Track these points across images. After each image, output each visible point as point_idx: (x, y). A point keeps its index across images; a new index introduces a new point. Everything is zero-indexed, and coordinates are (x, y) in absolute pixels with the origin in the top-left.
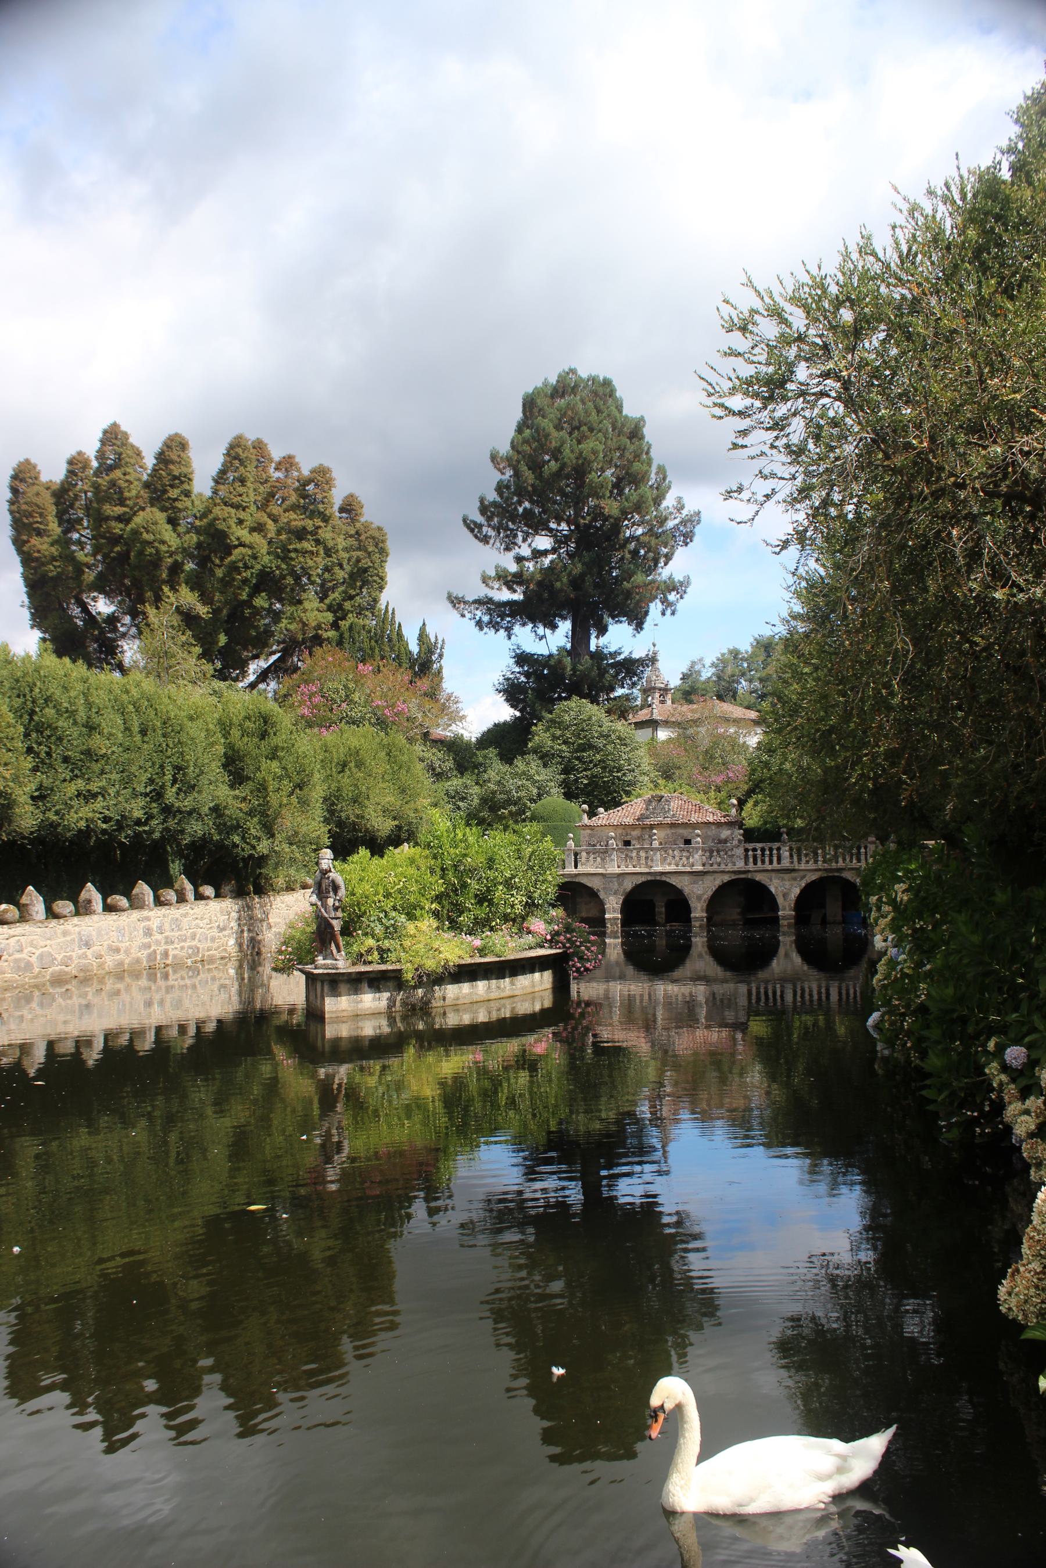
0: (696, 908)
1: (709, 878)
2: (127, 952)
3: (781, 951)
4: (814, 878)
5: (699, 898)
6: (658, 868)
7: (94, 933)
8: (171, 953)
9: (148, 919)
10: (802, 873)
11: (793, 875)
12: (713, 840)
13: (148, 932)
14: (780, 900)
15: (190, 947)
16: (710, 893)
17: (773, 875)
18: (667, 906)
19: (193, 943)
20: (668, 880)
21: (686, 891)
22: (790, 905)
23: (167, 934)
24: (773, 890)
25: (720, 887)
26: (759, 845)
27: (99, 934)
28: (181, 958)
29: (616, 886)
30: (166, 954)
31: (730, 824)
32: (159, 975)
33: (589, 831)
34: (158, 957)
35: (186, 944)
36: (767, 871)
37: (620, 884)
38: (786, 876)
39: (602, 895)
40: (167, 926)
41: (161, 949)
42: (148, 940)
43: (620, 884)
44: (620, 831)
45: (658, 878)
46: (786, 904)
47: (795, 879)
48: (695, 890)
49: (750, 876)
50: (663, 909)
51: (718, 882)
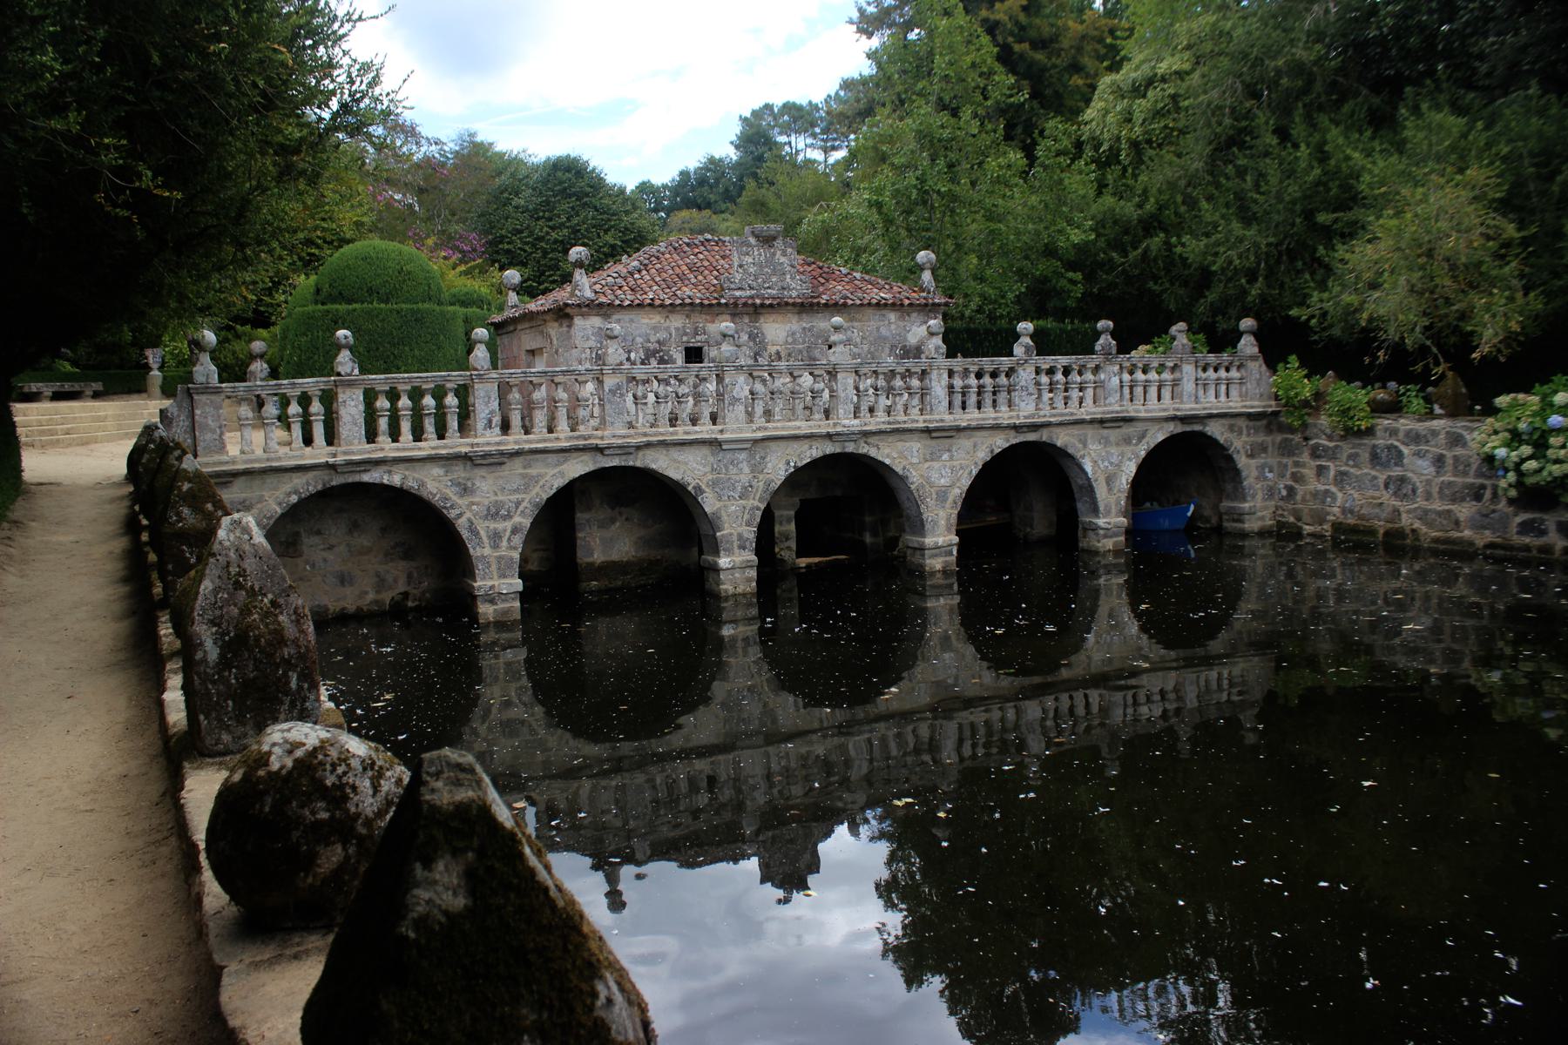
0: (935, 523)
1: (964, 443)
3: (1103, 610)
4: (1161, 437)
5: (942, 496)
6: (854, 424)
10: (1140, 427)
11: (1128, 430)
12: (893, 347)
14: (1101, 492)
16: (966, 482)
17: (1090, 432)
18: (799, 518)
20: (873, 453)
21: (915, 479)
22: (1118, 503)
24: (1088, 468)
25: (986, 466)
26: (1063, 360)
29: (743, 474)
31: (927, 309)
33: (596, 321)
36: (1081, 422)
37: (756, 469)
38: (1113, 434)
39: (709, 503)
43: (756, 469)
44: (677, 321)
45: (850, 448)
46: (1112, 499)
47: (1127, 441)
48: (934, 476)
49: (1044, 436)
50: (792, 527)
51: (983, 455)
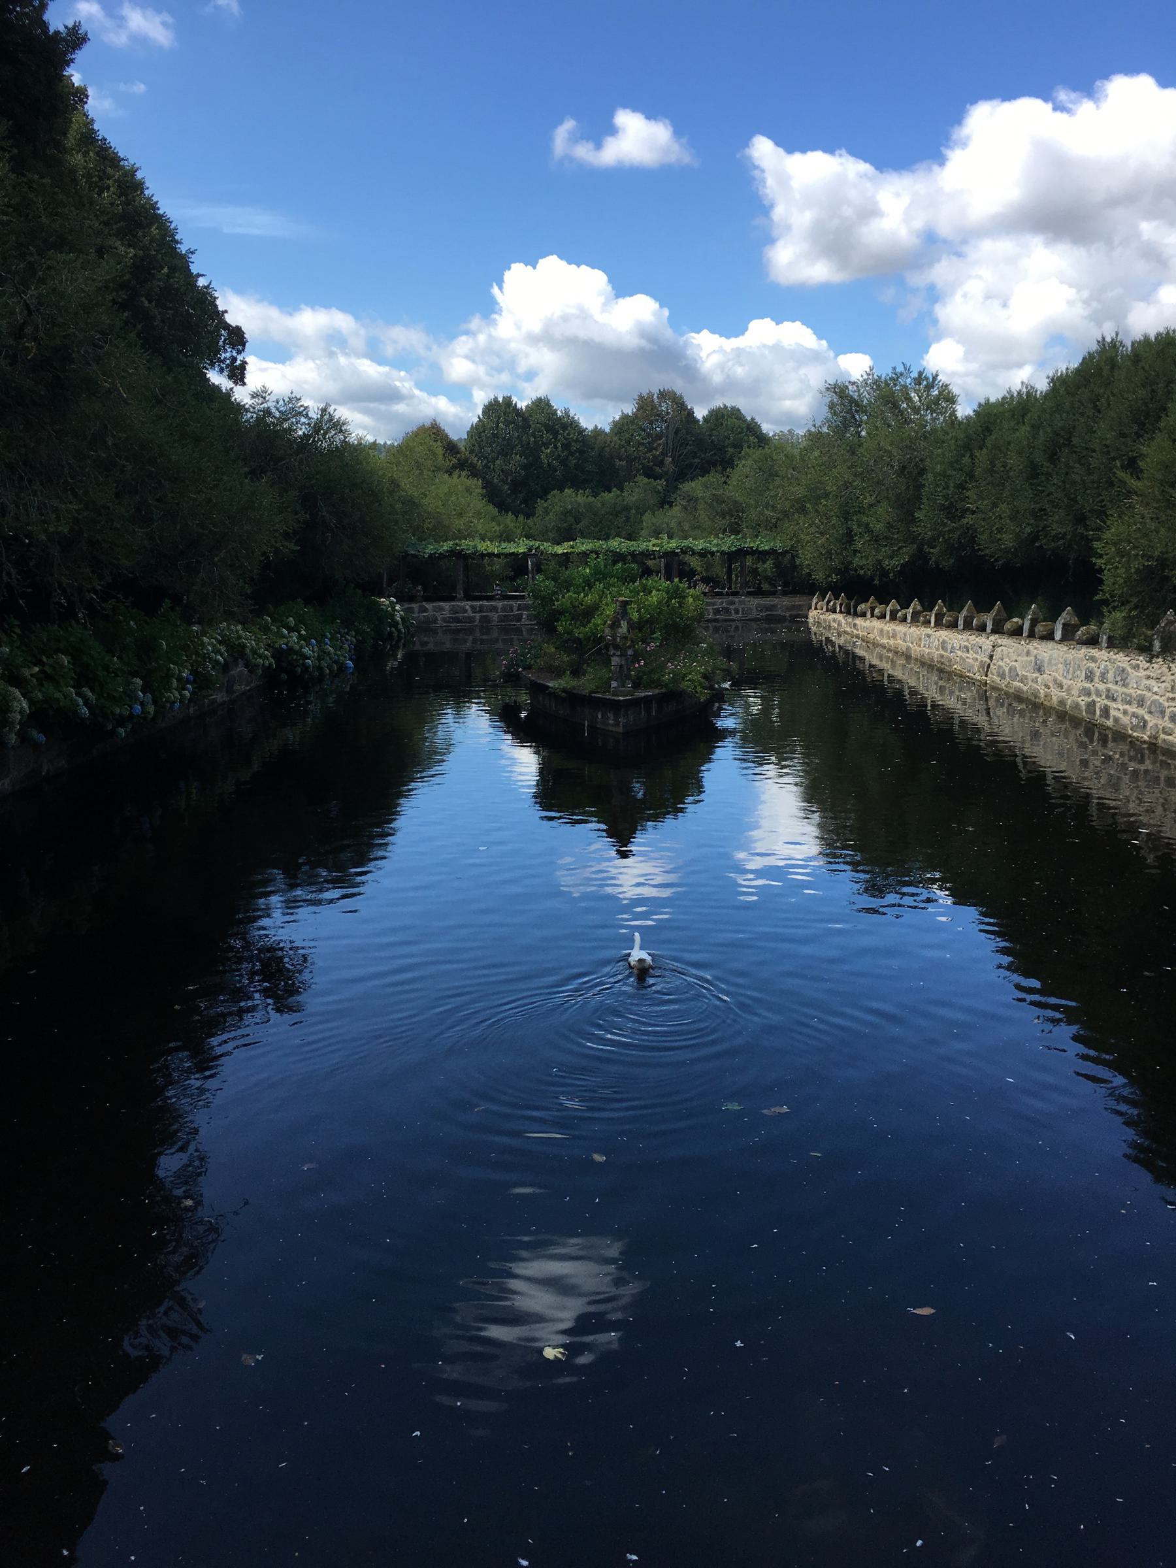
2: (1069, 690)
7: (1046, 660)
8: (1112, 713)
9: (1093, 659)
13: (1090, 677)
15: (1134, 715)
19: (1141, 712)
23: (1110, 686)
27: (1050, 660)
28: (1125, 727)
30: (1106, 711)
32: (1097, 734)
34: (1098, 712)
35: (1132, 709)
40: (1110, 676)
41: (1101, 702)
42: (1088, 685)
